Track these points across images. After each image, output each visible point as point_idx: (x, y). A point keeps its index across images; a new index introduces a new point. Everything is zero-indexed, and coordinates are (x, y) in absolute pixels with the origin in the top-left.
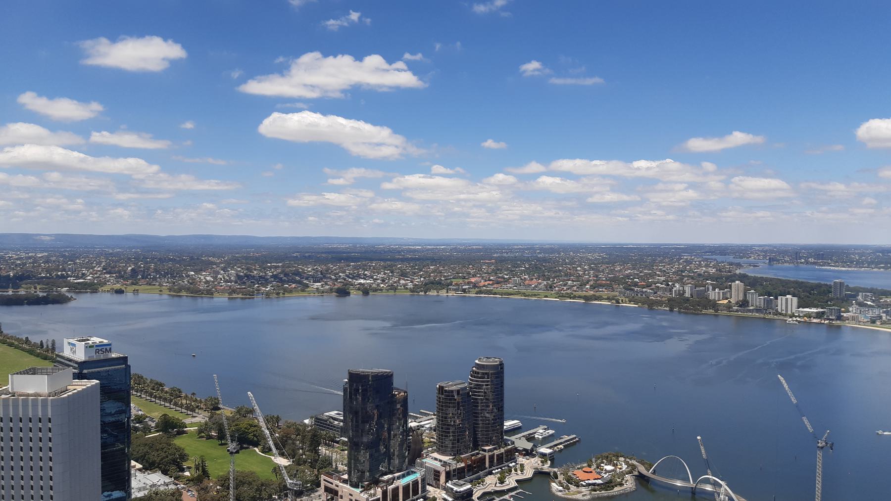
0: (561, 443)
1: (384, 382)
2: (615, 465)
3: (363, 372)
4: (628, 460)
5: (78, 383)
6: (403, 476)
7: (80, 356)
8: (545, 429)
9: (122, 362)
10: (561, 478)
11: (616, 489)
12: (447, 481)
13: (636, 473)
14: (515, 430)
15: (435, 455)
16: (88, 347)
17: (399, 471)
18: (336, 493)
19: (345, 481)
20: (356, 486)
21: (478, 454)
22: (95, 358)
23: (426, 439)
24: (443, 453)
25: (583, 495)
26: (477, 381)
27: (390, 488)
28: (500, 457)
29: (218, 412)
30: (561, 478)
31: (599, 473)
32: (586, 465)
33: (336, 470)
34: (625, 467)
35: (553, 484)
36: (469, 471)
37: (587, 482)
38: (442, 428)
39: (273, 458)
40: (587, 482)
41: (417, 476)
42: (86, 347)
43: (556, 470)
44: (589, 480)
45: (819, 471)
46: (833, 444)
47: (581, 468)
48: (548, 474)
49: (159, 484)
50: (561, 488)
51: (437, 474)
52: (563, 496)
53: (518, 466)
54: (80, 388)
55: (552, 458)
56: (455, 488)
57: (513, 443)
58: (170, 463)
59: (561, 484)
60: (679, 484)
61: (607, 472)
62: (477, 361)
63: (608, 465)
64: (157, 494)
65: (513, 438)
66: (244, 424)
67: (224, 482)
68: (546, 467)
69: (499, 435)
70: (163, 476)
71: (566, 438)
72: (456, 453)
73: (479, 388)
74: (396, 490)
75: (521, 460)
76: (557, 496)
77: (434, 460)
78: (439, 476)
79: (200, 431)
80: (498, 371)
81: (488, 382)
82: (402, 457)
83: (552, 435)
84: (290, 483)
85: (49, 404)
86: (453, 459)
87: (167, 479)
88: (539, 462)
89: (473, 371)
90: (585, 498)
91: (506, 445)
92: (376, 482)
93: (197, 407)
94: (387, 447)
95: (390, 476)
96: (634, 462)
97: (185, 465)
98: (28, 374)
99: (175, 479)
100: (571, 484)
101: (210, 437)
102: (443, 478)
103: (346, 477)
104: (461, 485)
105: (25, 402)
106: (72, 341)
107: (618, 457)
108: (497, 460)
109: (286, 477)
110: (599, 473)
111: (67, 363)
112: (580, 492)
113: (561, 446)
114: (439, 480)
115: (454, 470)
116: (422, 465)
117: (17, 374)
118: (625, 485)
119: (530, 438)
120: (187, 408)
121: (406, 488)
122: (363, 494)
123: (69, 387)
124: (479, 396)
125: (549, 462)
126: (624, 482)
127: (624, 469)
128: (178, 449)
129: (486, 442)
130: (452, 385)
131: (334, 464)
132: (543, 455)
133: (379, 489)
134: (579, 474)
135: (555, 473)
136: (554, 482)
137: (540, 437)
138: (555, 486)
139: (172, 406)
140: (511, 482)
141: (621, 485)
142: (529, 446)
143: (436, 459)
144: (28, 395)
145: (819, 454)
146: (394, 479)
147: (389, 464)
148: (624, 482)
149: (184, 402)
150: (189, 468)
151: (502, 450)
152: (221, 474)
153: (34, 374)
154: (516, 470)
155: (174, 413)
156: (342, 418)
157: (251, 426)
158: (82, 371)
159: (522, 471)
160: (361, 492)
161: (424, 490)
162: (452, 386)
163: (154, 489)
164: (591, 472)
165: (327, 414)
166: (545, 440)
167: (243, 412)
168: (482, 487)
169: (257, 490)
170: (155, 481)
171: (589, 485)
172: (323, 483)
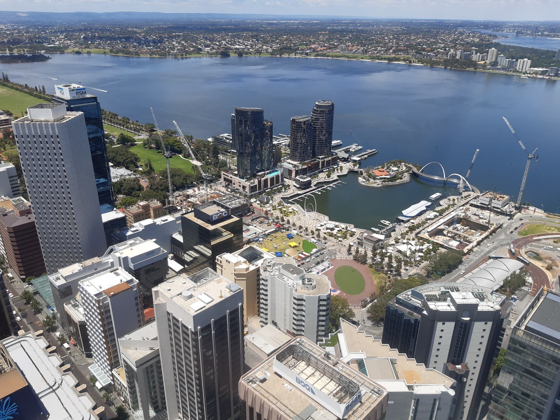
0: (366, 154)
1: (258, 116)
2: (399, 167)
3: (245, 109)
4: (407, 164)
5: (71, 114)
6: (270, 173)
7: (67, 96)
8: (357, 146)
9: (94, 100)
10: (365, 174)
11: (398, 181)
12: (296, 176)
13: (411, 172)
14: (338, 146)
15: (289, 161)
16: (71, 91)
17: (268, 170)
18: (231, 181)
19: (236, 175)
20: (243, 178)
21: (315, 160)
22: (77, 98)
23: (283, 151)
24: (294, 160)
26: (316, 116)
27: (263, 179)
28: (328, 162)
29: (154, 133)
30: (365, 174)
31: (388, 172)
32: (380, 167)
33: (230, 168)
34: (404, 168)
35: (360, 178)
36: (309, 170)
38: (294, 145)
39: (191, 161)
41: (279, 173)
42: (70, 90)
43: (362, 170)
45: (526, 172)
46: (538, 156)
47: (378, 169)
48: (357, 172)
49: (125, 174)
50: (364, 180)
51: (290, 172)
53: (339, 168)
54: (72, 117)
55: (360, 163)
56: (301, 180)
57: (336, 154)
58: (130, 163)
59: (364, 178)
60: (436, 178)
61: (393, 171)
62: (317, 103)
64: (125, 180)
65: (336, 151)
66: (171, 140)
67: (164, 174)
68: (356, 168)
69: (327, 148)
70: (126, 170)
71: (370, 151)
72: (302, 160)
73: (318, 121)
74: (266, 181)
75: (341, 164)
76: (362, 185)
77: (288, 164)
78: (291, 173)
79: (145, 144)
80: (331, 109)
81: (323, 116)
82: (269, 162)
83: (361, 149)
84: (205, 176)
85: (56, 126)
86: (300, 163)
87: (130, 172)
88: (352, 165)
89: (314, 109)
90: (379, 186)
91: (332, 155)
92: (254, 176)
93: (141, 129)
94: (261, 156)
95: (263, 173)
96: (411, 166)
97: (139, 164)
98: (38, 107)
99: (134, 172)
100: (371, 178)
101: (151, 148)
102: (293, 174)
103: (236, 172)
104: (305, 178)
105: (40, 125)
106: (60, 86)
107: (400, 162)
108: (326, 164)
109: (202, 172)
110: (388, 172)
111: (60, 101)
112: (375, 183)
113: (366, 156)
114: (291, 175)
115: (301, 170)
116: (281, 167)
117: (32, 108)
119: (347, 151)
120: (135, 130)
121: (272, 179)
122: (246, 183)
123: (65, 116)
124: (317, 125)
125: (358, 165)
126: (403, 177)
127: (404, 169)
128: (133, 155)
129: (321, 153)
130: (300, 119)
131: (228, 165)
132: (355, 161)
133: (256, 180)
134: (376, 172)
135: (361, 171)
136: (360, 177)
137: (353, 151)
138: (361, 179)
139: (125, 129)
140: (334, 176)
141: (401, 178)
142: (346, 156)
143: (290, 163)
144: (41, 121)
145: (528, 162)
146: (265, 174)
147: (262, 166)
149: (132, 126)
150: (141, 166)
151: (330, 158)
152: (161, 169)
153: (42, 108)
154: (337, 170)
155: (128, 133)
156: (231, 138)
157: (176, 142)
158: (71, 105)
159: (341, 170)
160: (246, 181)
161: (283, 181)
162: (301, 119)
163: (123, 178)
164: (384, 171)
165: (222, 135)
166: (356, 153)
167: (169, 133)
168: (317, 179)
169: (184, 179)
170: (123, 173)
171: (382, 178)
172: (222, 176)
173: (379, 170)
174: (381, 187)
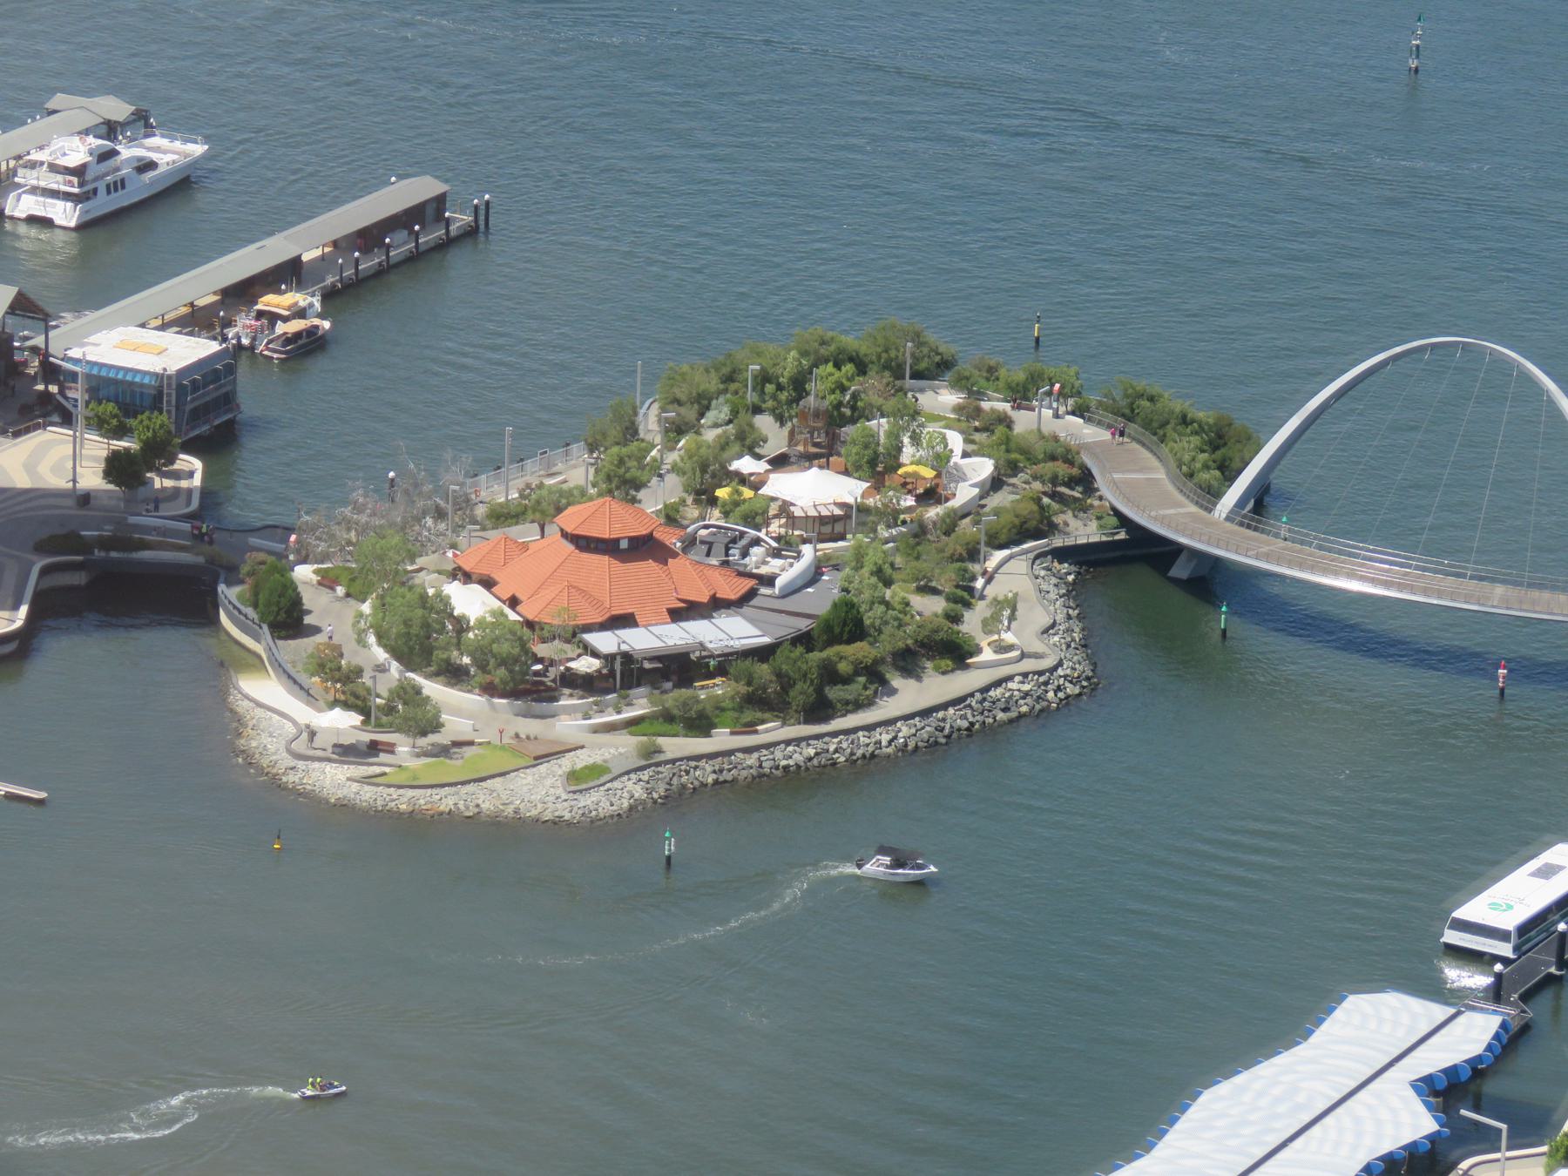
4: (995, 404)
8: (110, 129)
13: (1084, 531)
25: (573, 776)
32: (576, 470)
37: (605, 642)
40: (605, 642)
44: (623, 621)
50: (342, 722)
52: (368, 795)
63: (808, 459)
83: (183, 185)
90: (599, 802)
100: (454, 675)
118: (988, 655)
126: (971, 623)
127: (964, 494)
141: (957, 653)
148: (971, 623)
173: (572, 519)
174: (635, 820)
